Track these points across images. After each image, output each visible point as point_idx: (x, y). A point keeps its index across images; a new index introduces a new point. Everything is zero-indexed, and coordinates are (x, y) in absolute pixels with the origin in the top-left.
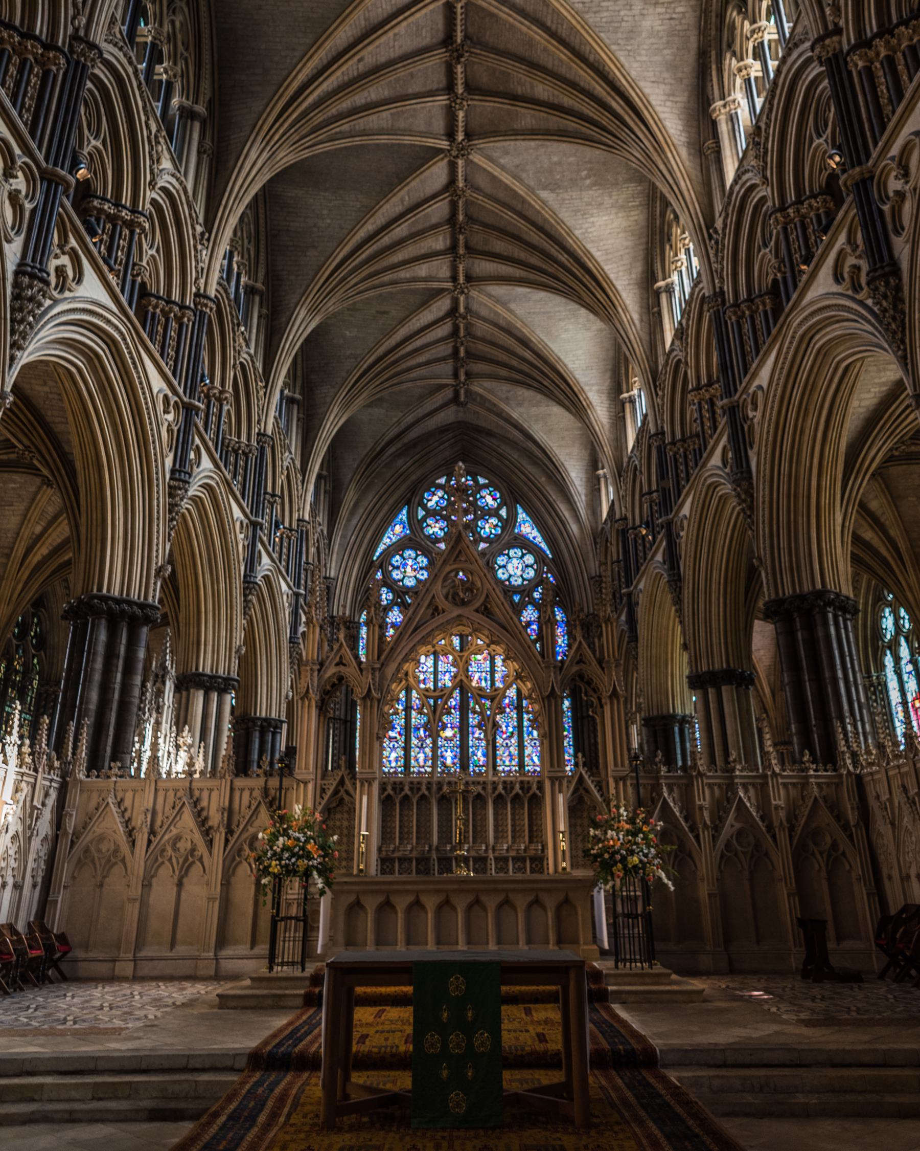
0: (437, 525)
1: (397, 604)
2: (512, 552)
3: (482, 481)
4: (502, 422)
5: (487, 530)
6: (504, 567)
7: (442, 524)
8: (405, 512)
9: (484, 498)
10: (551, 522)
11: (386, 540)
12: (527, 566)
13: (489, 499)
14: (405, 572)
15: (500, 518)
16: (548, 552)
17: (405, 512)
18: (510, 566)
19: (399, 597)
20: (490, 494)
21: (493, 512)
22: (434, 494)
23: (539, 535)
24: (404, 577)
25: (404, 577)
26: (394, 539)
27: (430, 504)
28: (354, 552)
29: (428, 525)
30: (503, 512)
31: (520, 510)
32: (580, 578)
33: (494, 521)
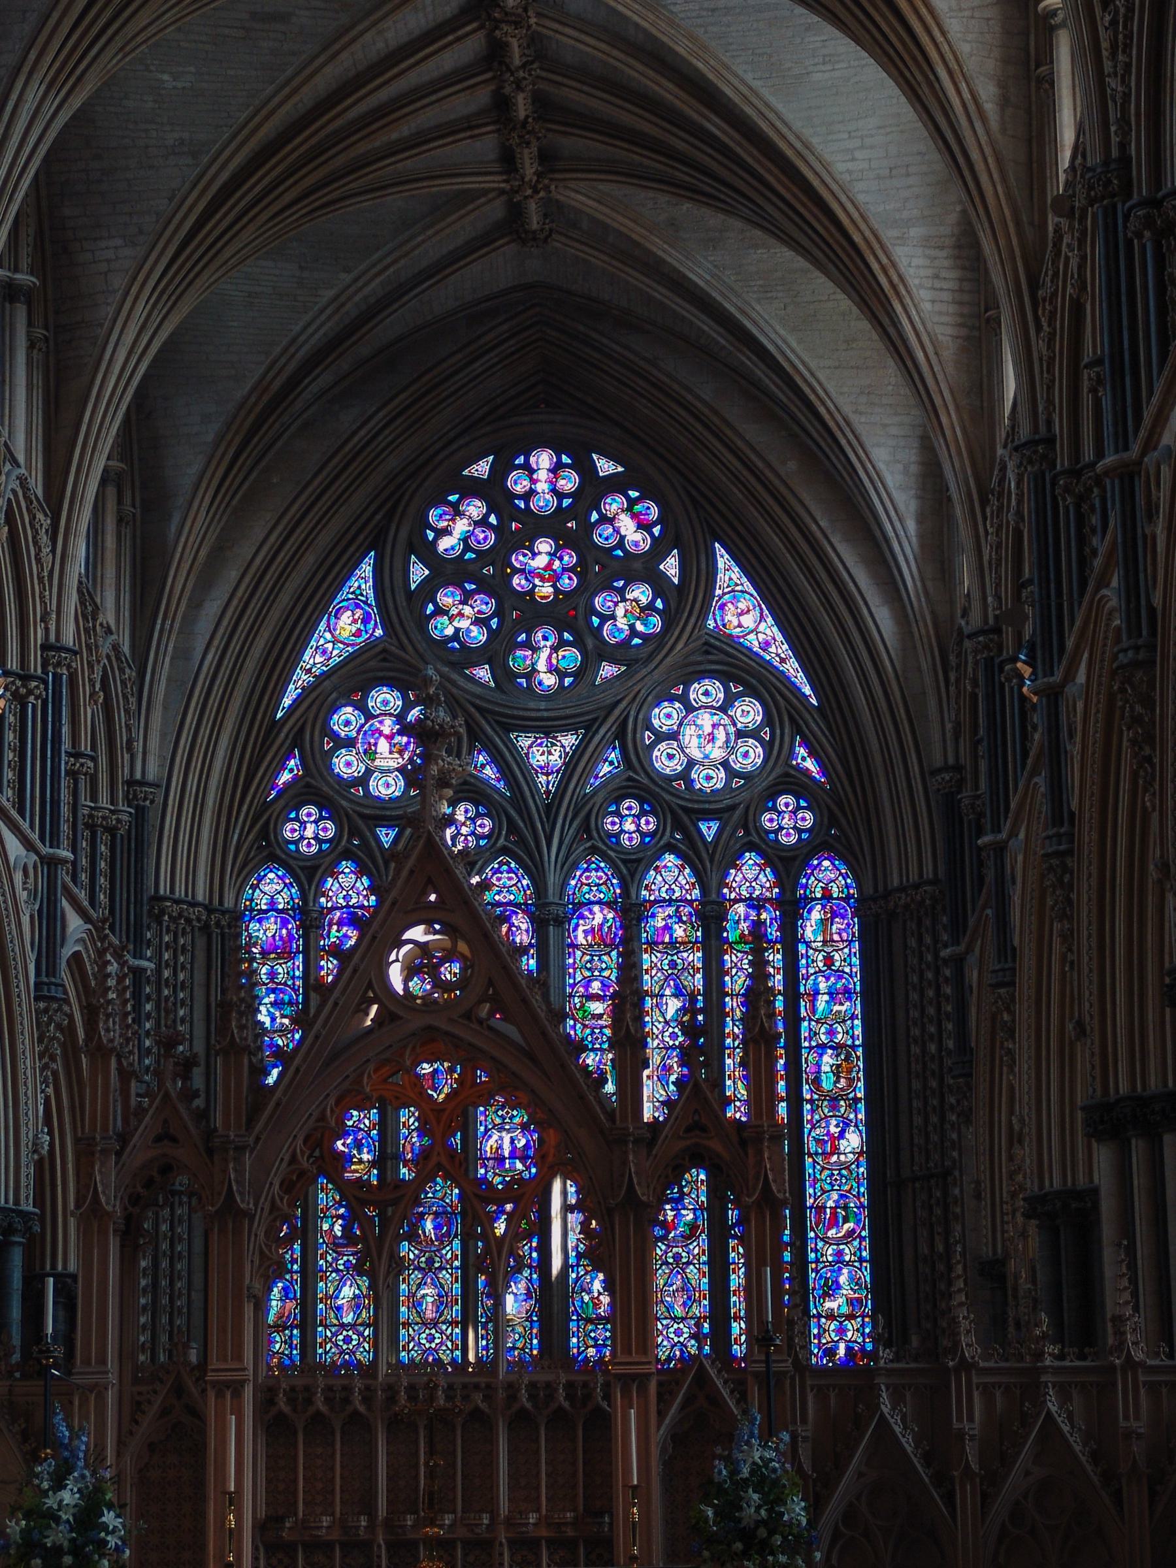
0: (467, 610)
1: (347, 855)
2: (696, 692)
3: (605, 467)
4: (660, 293)
5: (622, 623)
6: (674, 736)
7: (484, 605)
8: (366, 568)
9: (611, 521)
10: (813, 599)
11: (313, 660)
12: (740, 734)
13: (627, 525)
14: (370, 752)
15: (658, 583)
16: (807, 690)
17: (366, 568)
18: (689, 732)
19: (354, 832)
20: (630, 509)
21: (637, 565)
22: (458, 513)
23: (779, 637)
24: (369, 772)
25: (369, 772)
26: (337, 654)
27: (445, 544)
28: (214, 702)
29: (440, 611)
30: (671, 566)
31: (723, 559)
32: (900, 771)
33: (641, 593)
